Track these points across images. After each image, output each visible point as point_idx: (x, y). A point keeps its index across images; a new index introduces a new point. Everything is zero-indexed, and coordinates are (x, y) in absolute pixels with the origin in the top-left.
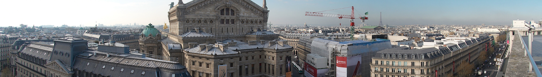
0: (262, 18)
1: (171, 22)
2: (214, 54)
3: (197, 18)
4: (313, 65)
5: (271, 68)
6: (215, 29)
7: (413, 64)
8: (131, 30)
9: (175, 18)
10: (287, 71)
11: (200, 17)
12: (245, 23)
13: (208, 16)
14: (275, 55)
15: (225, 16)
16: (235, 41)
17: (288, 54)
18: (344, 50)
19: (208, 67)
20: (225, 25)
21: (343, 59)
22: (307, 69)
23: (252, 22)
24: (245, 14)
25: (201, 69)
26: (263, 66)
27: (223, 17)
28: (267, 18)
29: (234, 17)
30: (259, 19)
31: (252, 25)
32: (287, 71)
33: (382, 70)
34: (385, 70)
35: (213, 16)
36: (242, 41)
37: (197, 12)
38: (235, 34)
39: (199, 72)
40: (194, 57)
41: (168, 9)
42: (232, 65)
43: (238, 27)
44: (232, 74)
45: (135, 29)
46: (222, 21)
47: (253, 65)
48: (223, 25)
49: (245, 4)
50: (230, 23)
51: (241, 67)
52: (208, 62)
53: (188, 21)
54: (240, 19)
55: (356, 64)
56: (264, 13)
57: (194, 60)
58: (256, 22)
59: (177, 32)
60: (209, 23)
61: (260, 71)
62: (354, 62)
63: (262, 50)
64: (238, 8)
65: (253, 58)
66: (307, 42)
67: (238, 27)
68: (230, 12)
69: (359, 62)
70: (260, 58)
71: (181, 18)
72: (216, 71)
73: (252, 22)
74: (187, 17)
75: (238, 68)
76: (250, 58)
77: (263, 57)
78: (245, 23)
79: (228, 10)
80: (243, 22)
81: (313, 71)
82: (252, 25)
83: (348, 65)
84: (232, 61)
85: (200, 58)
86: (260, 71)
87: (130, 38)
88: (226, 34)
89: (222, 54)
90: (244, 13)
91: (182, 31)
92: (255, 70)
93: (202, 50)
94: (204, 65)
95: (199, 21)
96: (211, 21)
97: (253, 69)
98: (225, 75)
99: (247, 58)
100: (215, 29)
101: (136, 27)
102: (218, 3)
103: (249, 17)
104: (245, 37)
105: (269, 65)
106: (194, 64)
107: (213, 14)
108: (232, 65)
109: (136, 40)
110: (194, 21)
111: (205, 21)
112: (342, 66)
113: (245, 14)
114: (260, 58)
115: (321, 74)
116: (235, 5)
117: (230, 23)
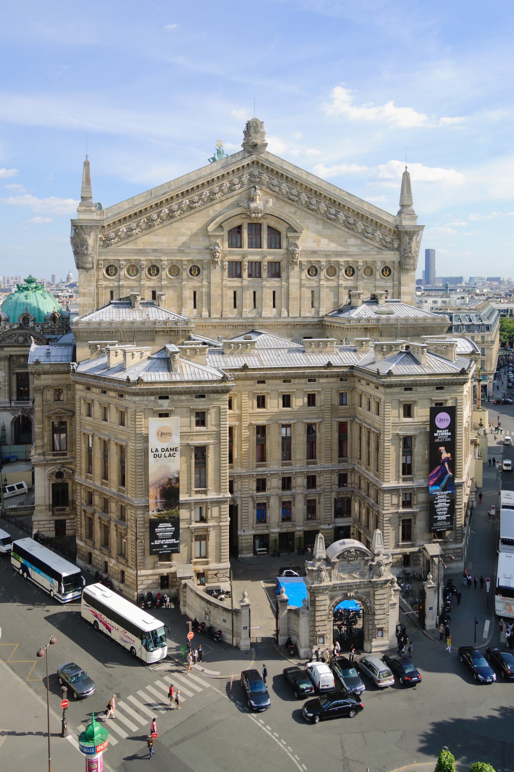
12: (323, 274)
31: (350, 284)
35: (199, 252)
37: (146, 238)
43: (294, 290)
46: (235, 270)
48: (236, 283)
49: (323, 207)
51: (261, 430)
53: (111, 269)
60: (185, 274)
65: (311, 400)
77: (351, 398)
80: (313, 270)
88: (248, 312)
95: (154, 269)
96: (195, 270)
99: (287, 401)
100: (209, 295)
116: (287, 211)
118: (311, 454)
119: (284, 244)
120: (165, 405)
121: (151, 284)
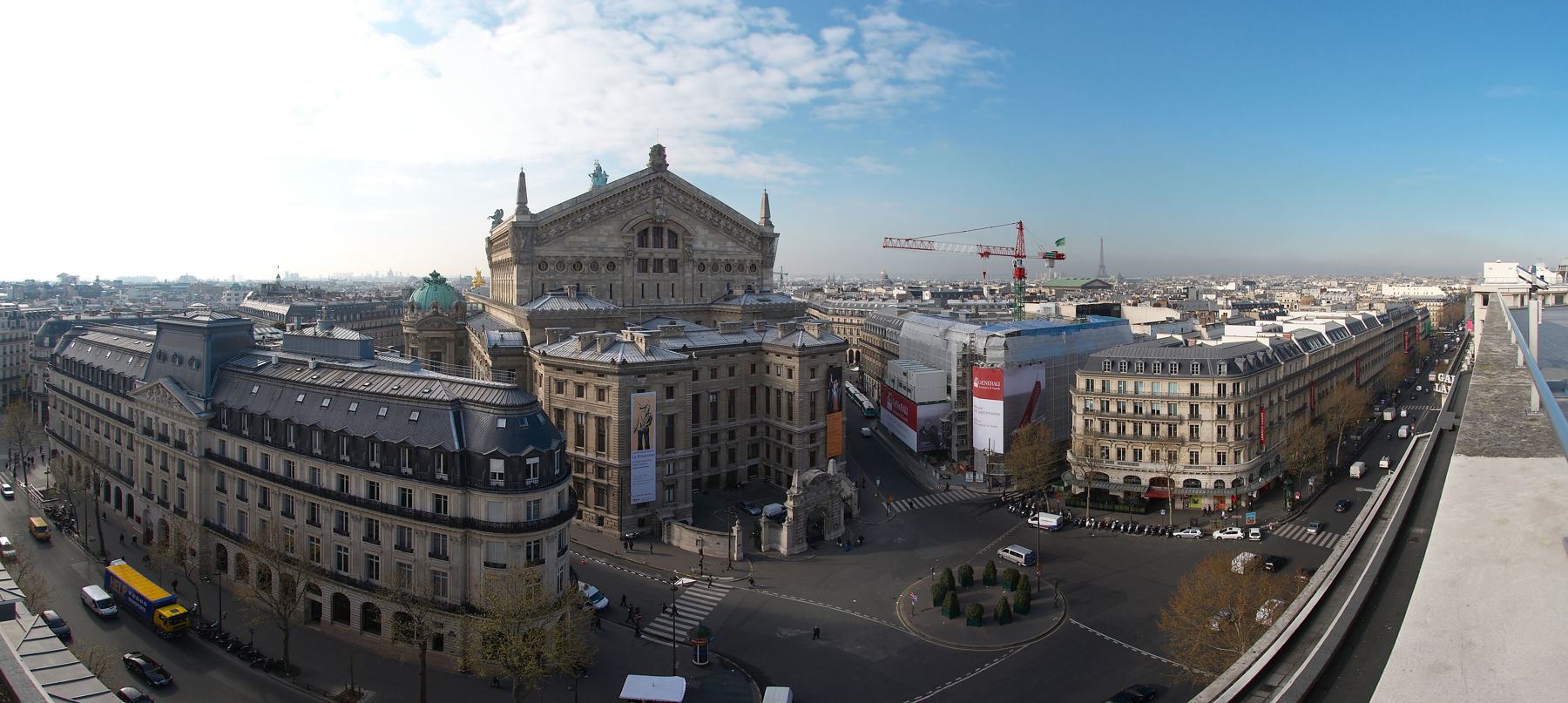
0: (756, 256)
1: (494, 266)
2: (618, 360)
3: (569, 256)
4: (904, 392)
5: (784, 402)
6: (622, 287)
7: (1194, 389)
8: (378, 291)
9: (507, 254)
10: (830, 409)
11: (577, 253)
12: (709, 270)
13: (601, 249)
14: (795, 363)
15: (651, 248)
16: (679, 323)
17: (833, 360)
18: (995, 348)
19: (601, 397)
20: (650, 276)
21: (993, 374)
22: (890, 405)
23: (728, 267)
24: (710, 245)
25: (581, 404)
26: (761, 394)
27: (644, 253)
28: (772, 257)
29: (676, 254)
30: (749, 257)
32: (830, 409)
33: (1105, 407)
34: (1113, 408)
35: (616, 250)
36: (698, 323)
37: (571, 238)
38: (680, 301)
39: (577, 414)
40: (560, 368)
41: (485, 229)
42: (670, 392)
43: (689, 282)
44: (671, 418)
45: (390, 289)
46: (643, 265)
47: (732, 392)
48: (644, 276)
49: (709, 215)
50: (666, 270)
51: (696, 398)
52: (603, 383)
53: (543, 264)
54: (695, 257)
55: (1030, 388)
56: (764, 240)
57: (561, 376)
58: (741, 267)
59: (512, 296)
60: (603, 269)
61: (753, 410)
62: (1024, 383)
63: (757, 349)
64: (687, 227)
65: (732, 372)
66: (889, 325)
67: (689, 282)
68: (666, 238)
69: (1038, 384)
70: (753, 371)
71: (524, 256)
72: (625, 409)
73: (728, 267)
74: (542, 251)
75: (689, 402)
76: (723, 372)
77: (760, 368)
78: (709, 270)
79: (658, 231)
81: (905, 410)
82: (728, 276)
83: (1008, 392)
84: (671, 380)
85: (580, 371)
86: (753, 410)
87: (375, 315)
89: (641, 360)
90: (705, 242)
91: (525, 292)
92: (738, 407)
93: (584, 349)
94: (591, 393)
95: (577, 265)
97: (732, 403)
98: (650, 420)
99: (714, 373)
100: (622, 287)
101: (390, 281)
102: (629, 213)
103: (720, 252)
104: (709, 311)
105: (779, 392)
106: (560, 390)
107: (618, 242)
108: (670, 392)
109: (394, 321)
110: (561, 264)
111: (594, 265)
112: (990, 395)
113: (710, 244)
114: (753, 371)
115: (927, 420)
116: (681, 218)
117: (666, 270)
118: (731, 414)
119: (681, 245)
120: (643, 381)
121: (576, 277)
